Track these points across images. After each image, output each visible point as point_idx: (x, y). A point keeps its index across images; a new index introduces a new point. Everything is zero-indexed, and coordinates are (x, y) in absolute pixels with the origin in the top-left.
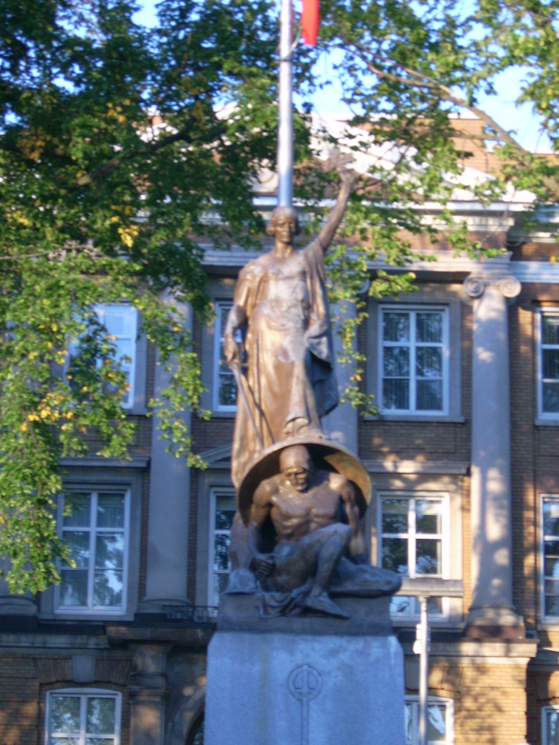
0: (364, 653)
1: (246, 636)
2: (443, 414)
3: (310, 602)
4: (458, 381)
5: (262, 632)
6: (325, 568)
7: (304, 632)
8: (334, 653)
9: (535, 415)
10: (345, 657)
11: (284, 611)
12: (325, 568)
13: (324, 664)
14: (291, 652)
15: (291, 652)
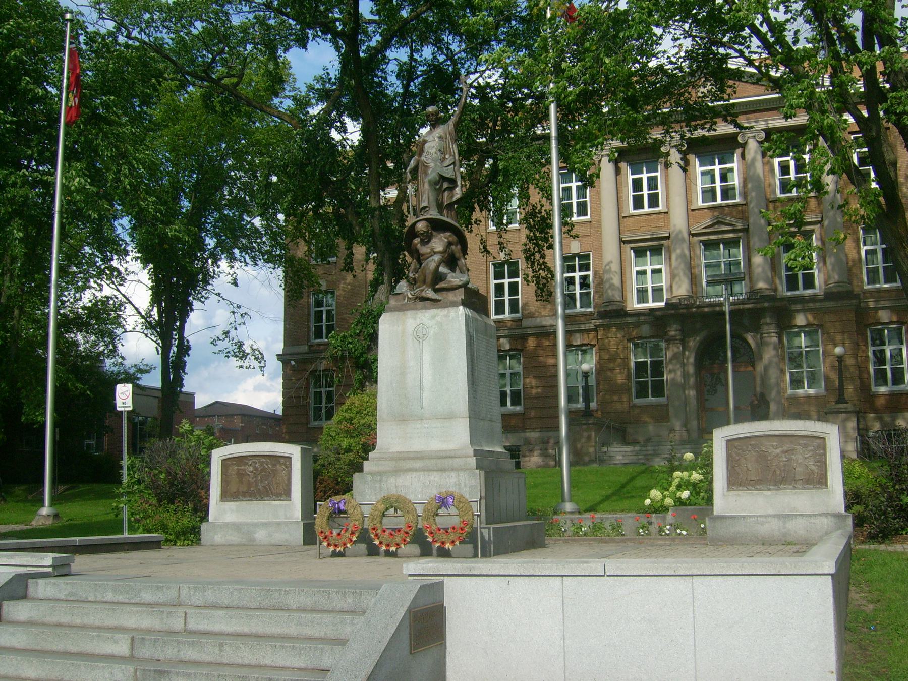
0: (447, 316)
1: (397, 313)
3: (424, 294)
5: (404, 311)
7: (422, 308)
8: (433, 317)
10: (438, 319)
14: (415, 319)
15: (415, 319)
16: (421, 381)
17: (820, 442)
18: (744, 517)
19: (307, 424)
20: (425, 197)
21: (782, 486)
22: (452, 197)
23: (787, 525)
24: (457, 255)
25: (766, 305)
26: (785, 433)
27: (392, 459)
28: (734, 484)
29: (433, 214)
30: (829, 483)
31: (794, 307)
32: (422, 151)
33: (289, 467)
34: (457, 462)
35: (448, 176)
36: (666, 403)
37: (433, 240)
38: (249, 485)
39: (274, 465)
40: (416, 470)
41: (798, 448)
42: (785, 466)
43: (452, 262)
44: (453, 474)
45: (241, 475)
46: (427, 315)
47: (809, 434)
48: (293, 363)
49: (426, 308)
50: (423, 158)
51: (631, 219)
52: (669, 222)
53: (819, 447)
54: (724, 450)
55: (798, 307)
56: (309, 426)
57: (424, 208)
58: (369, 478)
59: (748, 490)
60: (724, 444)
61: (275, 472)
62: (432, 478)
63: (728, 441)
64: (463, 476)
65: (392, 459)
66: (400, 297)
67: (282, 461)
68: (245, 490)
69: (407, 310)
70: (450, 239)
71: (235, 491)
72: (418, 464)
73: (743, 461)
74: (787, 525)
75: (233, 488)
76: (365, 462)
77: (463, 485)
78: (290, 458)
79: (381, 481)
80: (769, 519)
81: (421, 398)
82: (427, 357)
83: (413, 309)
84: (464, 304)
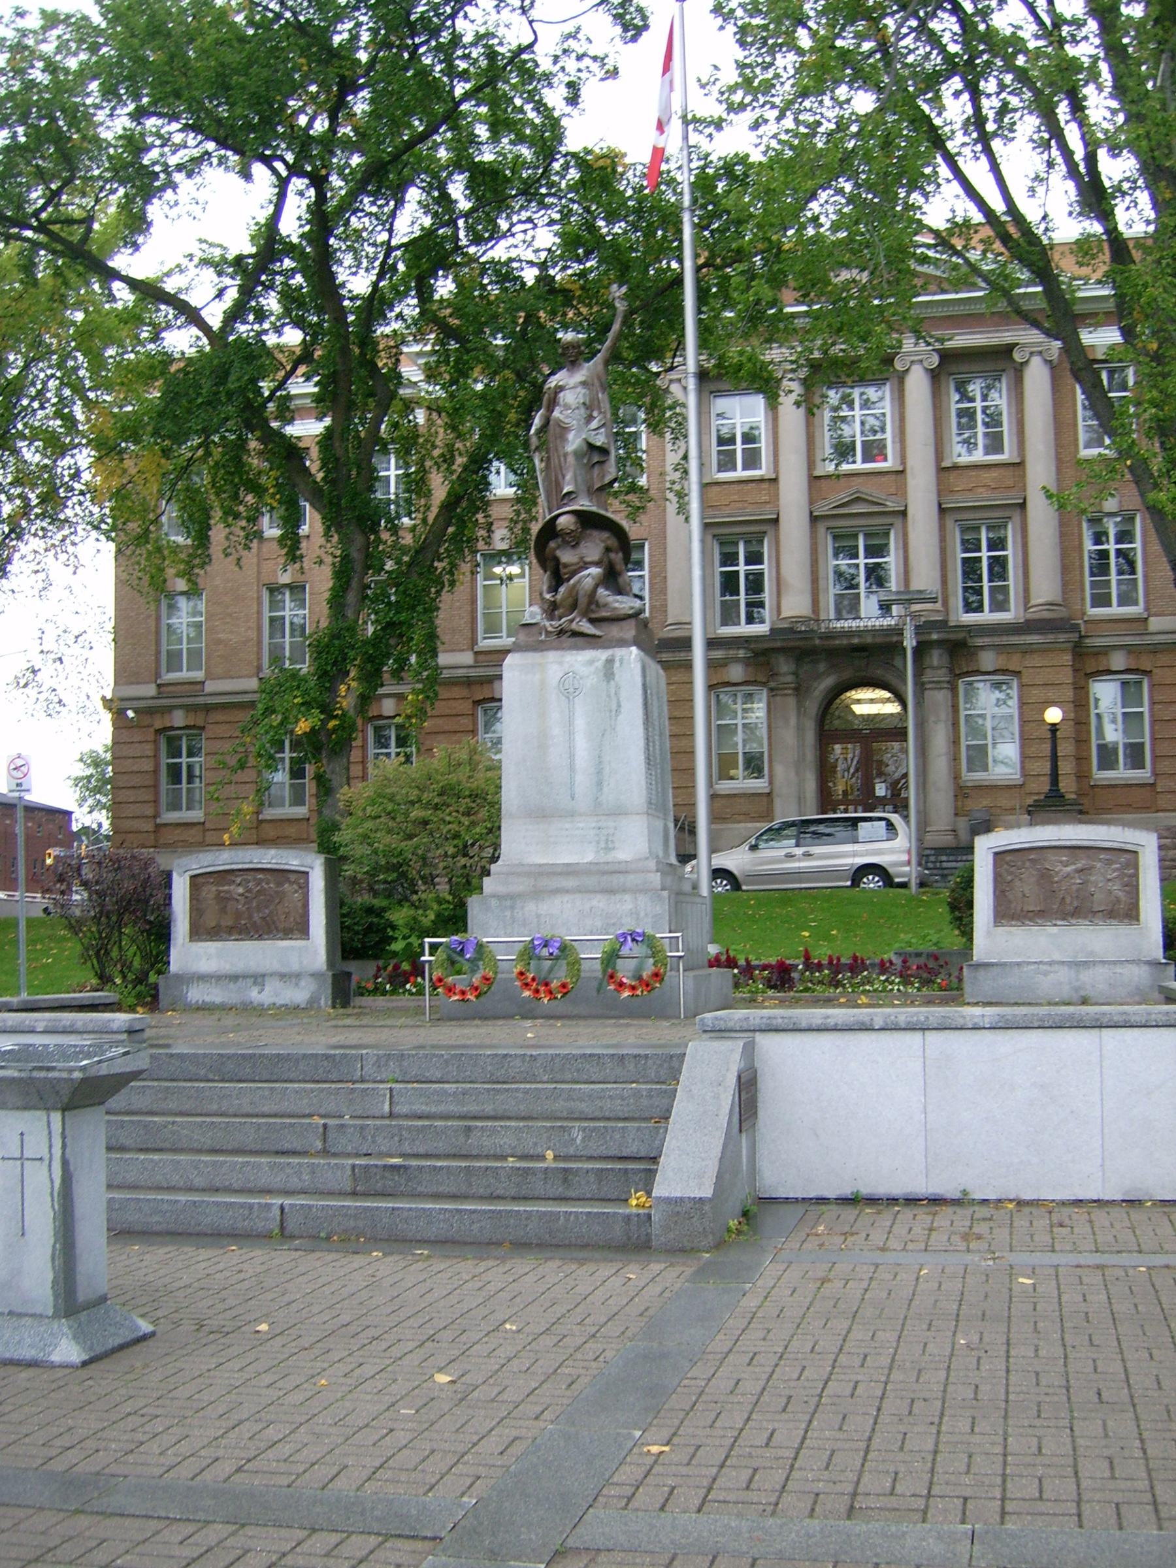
2: (887, 465)
3: (574, 626)
4: (1014, 430)
6: (583, 601)
7: (571, 648)
9: (1077, 451)
11: (561, 632)
12: (583, 601)
13: (584, 671)
14: (561, 663)
16: (572, 757)
17: (1130, 856)
18: (1018, 964)
19: (155, 817)
20: (568, 477)
21: (1074, 921)
23: (1081, 976)
25: (935, 637)
26: (1079, 843)
27: (528, 874)
28: (1003, 917)
29: (584, 504)
30: (1142, 917)
31: (979, 642)
32: (553, 403)
33: (305, 888)
34: (631, 880)
37: (582, 545)
38: (238, 915)
39: (279, 884)
40: (567, 891)
41: (1099, 865)
43: (612, 578)
44: (627, 897)
45: (223, 900)
47: (1116, 845)
48: (130, 714)
49: (577, 648)
50: (556, 414)
51: (716, 489)
52: (777, 495)
53: (1127, 865)
54: (991, 867)
55: (987, 641)
56: (158, 821)
57: (569, 493)
58: (494, 902)
59: (1024, 925)
60: (991, 858)
61: (281, 896)
62: (595, 903)
63: (996, 854)
64: (643, 901)
65: (528, 874)
66: (535, 630)
67: (292, 877)
68: (230, 923)
70: (609, 542)
71: (213, 924)
72: (570, 883)
73: (1017, 883)
74: (1081, 976)
75: (210, 920)
76: (485, 879)
77: (642, 914)
79: (512, 908)
80: (1056, 967)
83: (557, 649)
84: (637, 643)
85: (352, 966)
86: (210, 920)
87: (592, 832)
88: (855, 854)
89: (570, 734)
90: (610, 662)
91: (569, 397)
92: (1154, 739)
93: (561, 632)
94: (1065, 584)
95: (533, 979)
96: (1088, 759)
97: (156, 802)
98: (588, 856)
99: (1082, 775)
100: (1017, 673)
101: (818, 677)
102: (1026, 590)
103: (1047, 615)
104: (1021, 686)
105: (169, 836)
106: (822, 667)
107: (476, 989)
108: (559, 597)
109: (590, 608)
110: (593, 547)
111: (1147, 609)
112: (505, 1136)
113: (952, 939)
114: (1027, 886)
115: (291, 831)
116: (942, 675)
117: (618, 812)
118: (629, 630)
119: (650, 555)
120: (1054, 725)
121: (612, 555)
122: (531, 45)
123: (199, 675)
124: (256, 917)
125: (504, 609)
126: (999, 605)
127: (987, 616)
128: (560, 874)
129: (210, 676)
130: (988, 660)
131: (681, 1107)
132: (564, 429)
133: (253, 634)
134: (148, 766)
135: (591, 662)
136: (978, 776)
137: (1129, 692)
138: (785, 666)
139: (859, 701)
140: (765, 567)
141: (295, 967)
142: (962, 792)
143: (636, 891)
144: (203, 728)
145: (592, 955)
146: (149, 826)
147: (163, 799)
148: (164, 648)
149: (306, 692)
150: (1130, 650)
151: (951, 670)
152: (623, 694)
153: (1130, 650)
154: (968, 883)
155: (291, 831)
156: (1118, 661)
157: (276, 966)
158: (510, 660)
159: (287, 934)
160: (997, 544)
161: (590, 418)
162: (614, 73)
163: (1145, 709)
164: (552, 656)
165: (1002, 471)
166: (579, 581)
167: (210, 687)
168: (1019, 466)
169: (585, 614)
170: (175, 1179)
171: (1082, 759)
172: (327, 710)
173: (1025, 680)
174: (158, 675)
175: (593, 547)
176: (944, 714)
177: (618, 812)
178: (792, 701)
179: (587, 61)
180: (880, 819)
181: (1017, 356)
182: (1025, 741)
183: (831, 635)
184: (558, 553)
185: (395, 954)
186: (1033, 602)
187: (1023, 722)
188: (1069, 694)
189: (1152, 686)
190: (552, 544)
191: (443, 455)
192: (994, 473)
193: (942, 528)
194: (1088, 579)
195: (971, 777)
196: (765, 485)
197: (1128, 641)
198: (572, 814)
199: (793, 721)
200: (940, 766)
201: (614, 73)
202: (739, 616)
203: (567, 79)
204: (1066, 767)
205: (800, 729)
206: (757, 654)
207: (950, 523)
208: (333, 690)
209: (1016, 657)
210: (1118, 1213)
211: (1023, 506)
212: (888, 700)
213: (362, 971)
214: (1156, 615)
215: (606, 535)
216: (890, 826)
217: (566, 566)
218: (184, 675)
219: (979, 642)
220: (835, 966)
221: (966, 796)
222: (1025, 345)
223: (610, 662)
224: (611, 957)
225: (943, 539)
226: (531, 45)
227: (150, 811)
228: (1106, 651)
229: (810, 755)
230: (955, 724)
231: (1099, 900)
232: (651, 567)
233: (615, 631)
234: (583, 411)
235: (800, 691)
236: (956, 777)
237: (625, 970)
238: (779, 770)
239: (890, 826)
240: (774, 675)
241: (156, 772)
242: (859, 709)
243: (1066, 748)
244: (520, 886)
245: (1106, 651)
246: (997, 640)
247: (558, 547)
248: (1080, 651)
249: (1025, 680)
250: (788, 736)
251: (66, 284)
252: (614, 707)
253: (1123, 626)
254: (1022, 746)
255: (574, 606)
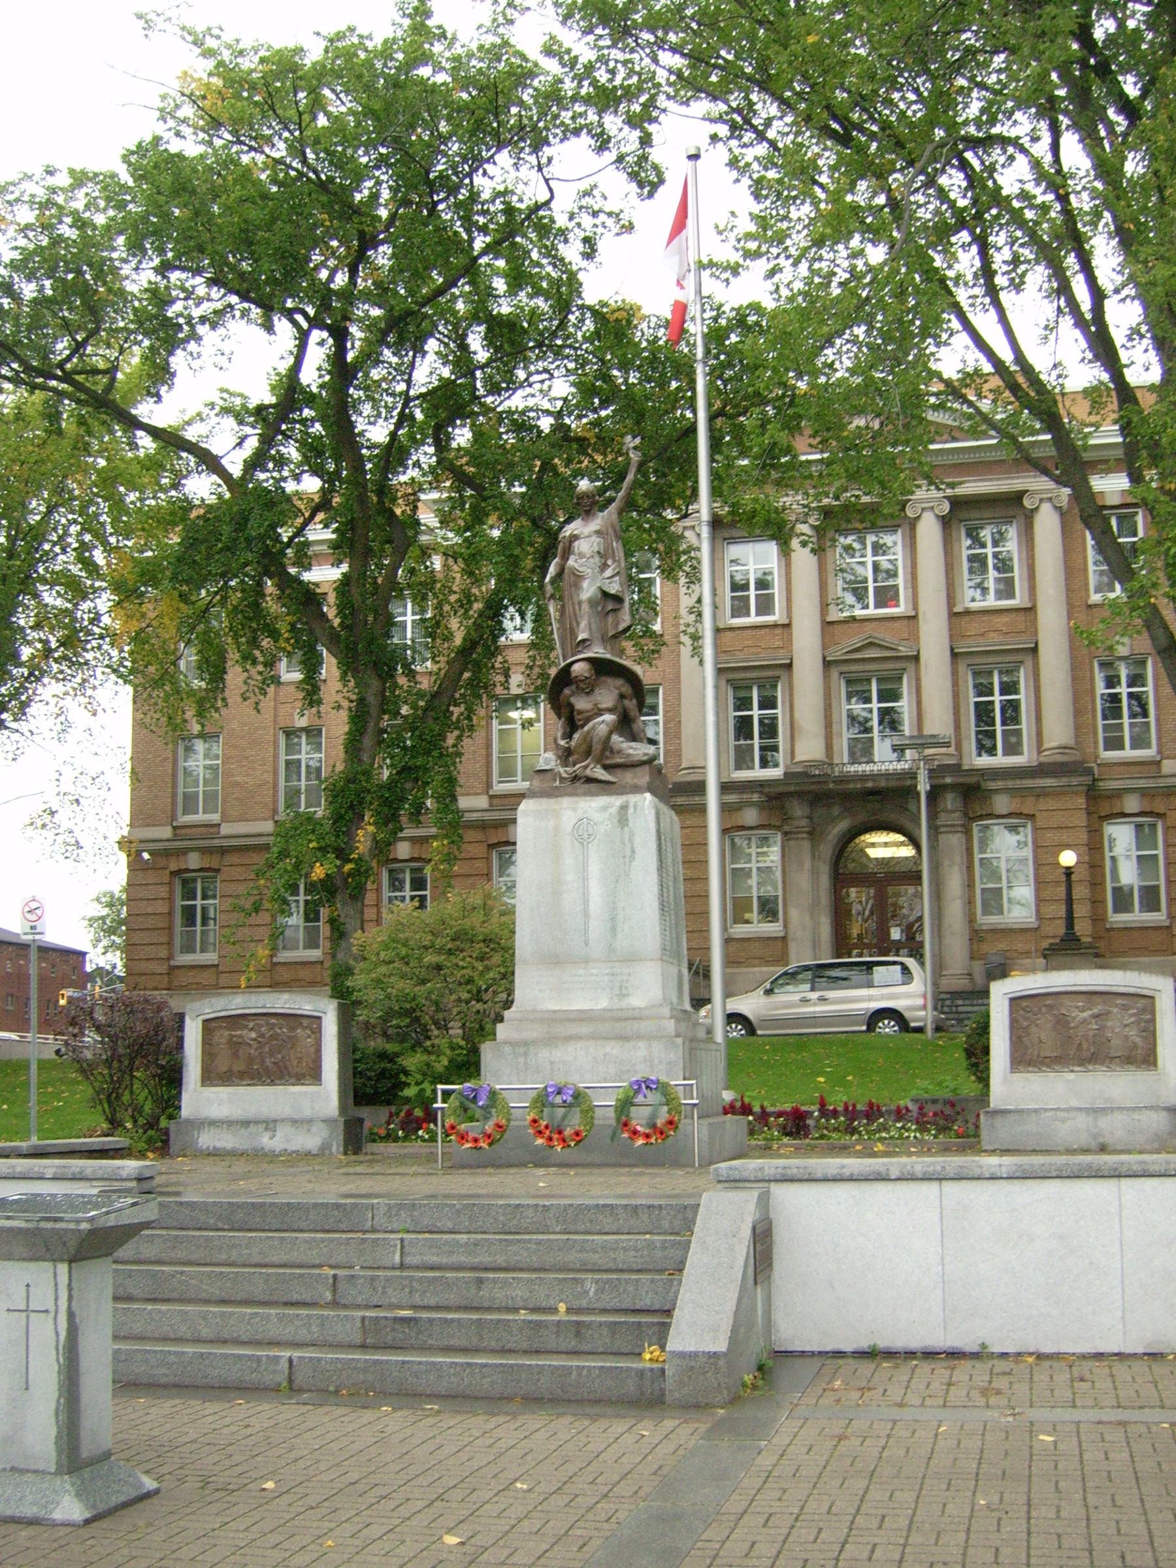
2: (901, 609)
3: (588, 772)
4: (1025, 576)
6: (597, 747)
7: (585, 794)
9: (1088, 596)
11: (575, 778)
12: (597, 747)
13: (597, 817)
14: (575, 810)
16: (586, 903)
18: (1036, 1111)
19: (168, 959)
20: (583, 624)
22: (617, 624)
24: (632, 714)
25: (948, 780)
27: (542, 1021)
28: (1020, 1063)
29: (598, 651)
31: (993, 785)
32: (568, 552)
34: (645, 1027)
35: (613, 592)
36: (782, 934)
37: (597, 691)
38: (250, 1060)
39: (292, 1029)
40: (579, 1038)
41: (1115, 1010)
42: (1095, 1036)
43: (626, 725)
44: (641, 1044)
45: (235, 1045)
46: (593, 804)
47: (1132, 990)
48: (146, 856)
50: (571, 562)
51: (728, 634)
52: (790, 640)
53: (1144, 1010)
54: (1006, 1012)
55: (999, 784)
56: (172, 963)
57: (583, 641)
58: (507, 1049)
59: (1041, 1071)
60: (1006, 1003)
61: (294, 1040)
62: (608, 1049)
63: (1012, 1000)
65: (542, 1021)
66: (549, 776)
67: (305, 1022)
68: (242, 1068)
69: (562, 796)
70: (623, 689)
71: (225, 1069)
72: (585, 1029)
73: (1034, 1029)
75: (222, 1064)
76: (499, 1026)
78: (319, 1018)
79: (526, 1054)
80: (1073, 1114)
81: (586, 930)
82: (594, 868)
83: (571, 795)
85: (364, 1112)
86: (222, 1064)
87: (606, 978)
88: (870, 999)
89: (584, 879)
90: (624, 808)
91: (584, 546)
92: (1169, 882)
93: (575, 778)
94: (1077, 728)
95: (547, 1127)
96: (1103, 902)
97: (170, 944)
98: (603, 1003)
99: (1098, 918)
100: (1031, 817)
101: (833, 820)
102: (1039, 734)
103: (1059, 758)
104: (1035, 829)
105: (183, 978)
106: (836, 811)
107: (489, 1136)
108: (573, 743)
109: (604, 754)
110: (607, 695)
111: (1159, 752)
112: (517, 1288)
113: (968, 1087)
114: (1043, 1032)
115: (304, 974)
116: (956, 818)
117: (632, 958)
118: (643, 777)
119: (665, 700)
120: (1068, 868)
121: (626, 702)
122: (547, 203)
123: (215, 817)
124: (269, 1062)
125: (519, 754)
126: (1012, 748)
127: (1000, 760)
128: (574, 1020)
129: (225, 818)
130: (1002, 804)
131: (695, 1259)
132: (578, 577)
133: (269, 778)
134: (162, 908)
135: (605, 808)
136: (993, 920)
137: (1143, 836)
138: (798, 810)
139: (873, 845)
140: (778, 711)
141: (307, 1112)
142: (976, 935)
143: (649, 1038)
144: (218, 871)
145: (605, 1102)
146: (163, 969)
147: (177, 943)
148: (181, 790)
149: (321, 837)
150: (1144, 793)
151: (966, 815)
152: (638, 840)
153: (1144, 793)
154: (984, 1028)
155: (304, 974)
156: (1132, 804)
157: (288, 1111)
158: (525, 806)
159: (299, 1079)
160: (1009, 688)
161: (604, 567)
162: (629, 228)
163: (1160, 852)
164: (566, 801)
165: (1013, 616)
166: (593, 728)
167: (225, 829)
168: (1030, 611)
169: (599, 761)
170: (184, 1330)
171: (1097, 902)
172: (342, 854)
173: (1039, 824)
174: (174, 817)
175: (607, 695)
176: (958, 858)
177: (632, 958)
178: (806, 845)
179: (602, 217)
180: (895, 963)
181: (1027, 503)
182: (1040, 884)
183: (845, 779)
184: (573, 700)
185: (407, 1100)
186: (1046, 745)
187: (1038, 865)
188: (1083, 836)
189: (1166, 829)
190: (567, 691)
191: (459, 600)
192: (1005, 619)
193: (954, 673)
194: (1100, 723)
195: (987, 921)
196: (778, 631)
197: (1142, 784)
198: (586, 961)
199: (807, 864)
200: (955, 910)
201: (629, 228)
202: (753, 760)
203: (582, 235)
204: (1080, 910)
205: (815, 873)
206: (771, 798)
207: (962, 667)
208: (351, 836)
209: (1030, 801)
210: (1139, 1367)
211: (1035, 650)
212: (902, 844)
213: (374, 1118)
214: (1168, 758)
215: (620, 682)
216: (905, 970)
217: (580, 712)
218: (201, 817)
219: (993, 785)
220: (851, 1113)
221: (981, 940)
222: (1035, 492)
223: (624, 808)
224: (625, 1105)
225: (955, 684)
226: (547, 203)
227: (163, 953)
228: (1119, 794)
229: (825, 898)
230: (970, 868)
231: (1116, 1046)
232: (665, 712)
233: (628, 777)
234: (597, 559)
235: (814, 834)
236: (971, 920)
237: (639, 1117)
238: (794, 913)
239: (905, 970)
240: (786, 819)
241: (170, 914)
242: (873, 853)
243: (1080, 892)
244: (533, 1032)
245: (1119, 794)
246: (1010, 784)
247: (573, 694)
248: (1093, 794)
249: (1039, 824)
250: (803, 880)
251: (89, 433)
252: (628, 853)
253: (1137, 768)
254: (1037, 890)
255: (588, 753)
